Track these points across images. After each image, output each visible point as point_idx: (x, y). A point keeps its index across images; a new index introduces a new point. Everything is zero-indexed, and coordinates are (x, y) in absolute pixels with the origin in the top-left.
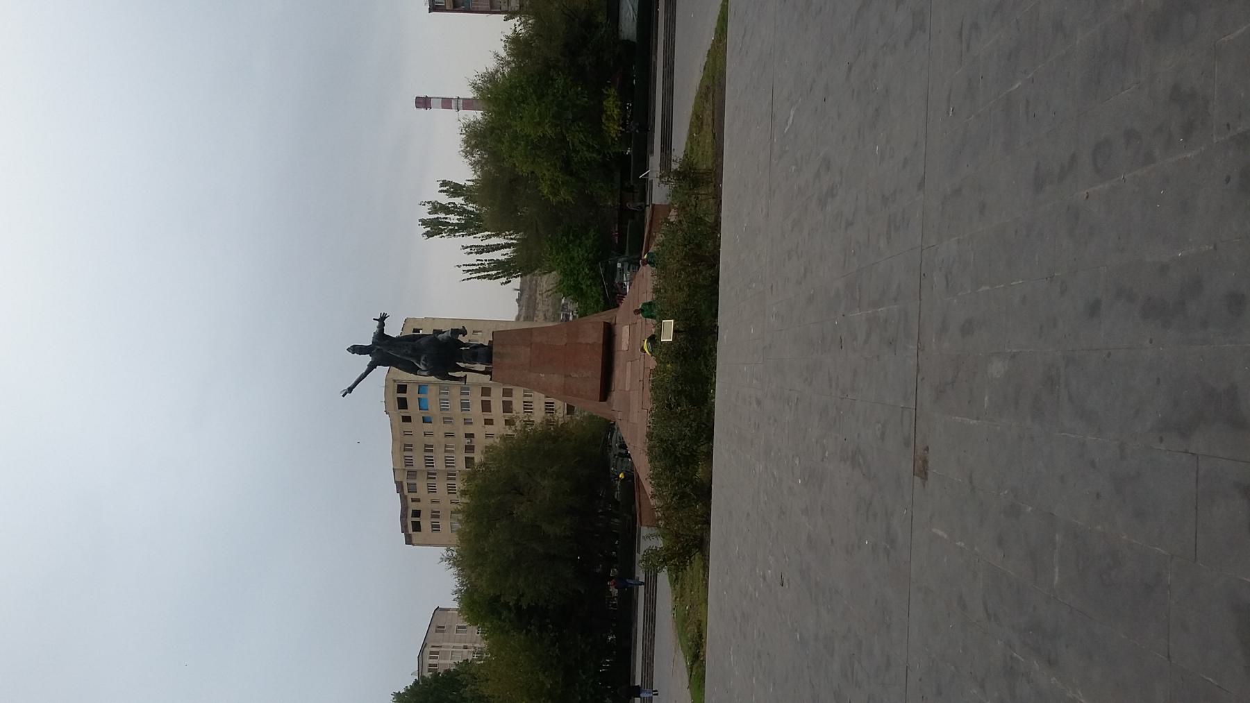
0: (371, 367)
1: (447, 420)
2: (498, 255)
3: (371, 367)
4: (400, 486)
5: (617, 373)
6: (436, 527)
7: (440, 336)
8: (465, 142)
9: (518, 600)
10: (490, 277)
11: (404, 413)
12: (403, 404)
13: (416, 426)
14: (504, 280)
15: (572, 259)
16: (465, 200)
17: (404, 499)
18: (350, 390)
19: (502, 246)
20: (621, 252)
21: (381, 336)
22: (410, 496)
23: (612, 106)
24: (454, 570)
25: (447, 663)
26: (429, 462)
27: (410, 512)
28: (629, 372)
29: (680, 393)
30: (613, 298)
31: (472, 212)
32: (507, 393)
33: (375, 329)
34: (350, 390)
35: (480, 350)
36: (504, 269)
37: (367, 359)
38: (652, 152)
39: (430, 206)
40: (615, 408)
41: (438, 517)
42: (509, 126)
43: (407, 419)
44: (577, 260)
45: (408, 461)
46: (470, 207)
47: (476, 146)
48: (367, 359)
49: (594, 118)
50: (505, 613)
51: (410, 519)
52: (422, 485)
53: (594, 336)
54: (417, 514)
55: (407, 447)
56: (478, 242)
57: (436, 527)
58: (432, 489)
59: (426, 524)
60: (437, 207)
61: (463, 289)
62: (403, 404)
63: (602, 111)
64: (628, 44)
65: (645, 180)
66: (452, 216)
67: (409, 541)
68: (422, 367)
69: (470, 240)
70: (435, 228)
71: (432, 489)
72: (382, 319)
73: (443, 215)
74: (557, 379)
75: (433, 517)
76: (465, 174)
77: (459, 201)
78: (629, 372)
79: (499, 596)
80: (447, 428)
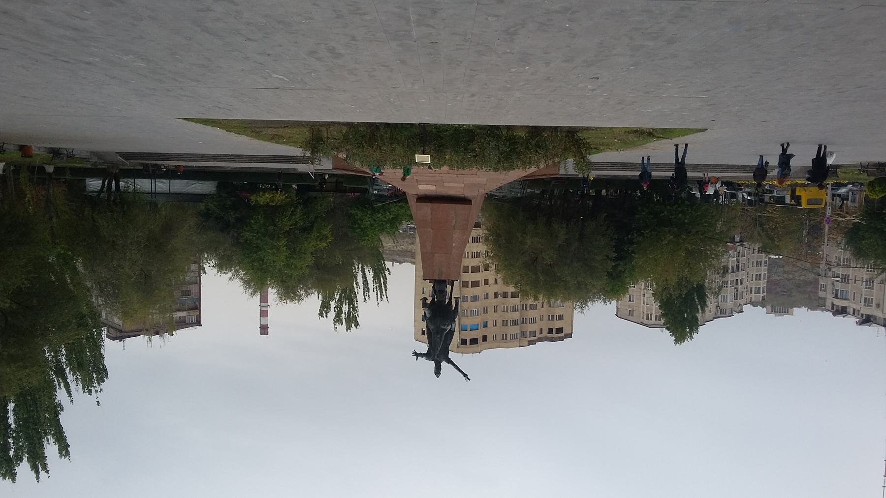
0: (449, 361)
1: (485, 311)
2: (370, 277)
3: (449, 361)
5: (452, 193)
6: (560, 318)
7: (428, 315)
8: (292, 300)
9: (611, 259)
10: (385, 282)
11: (480, 340)
12: (474, 341)
13: (490, 332)
14: (387, 273)
15: (371, 225)
16: (332, 300)
17: (540, 340)
18: (465, 375)
19: (363, 274)
20: (366, 190)
21: (428, 356)
22: (538, 335)
23: (263, 199)
24: (589, 304)
25: (655, 308)
26: (514, 323)
27: (550, 335)
28: (451, 185)
29: (466, 149)
30: (399, 197)
31: (341, 295)
32: (466, 270)
33: (424, 359)
34: (465, 375)
35: (437, 288)
36: (380, 273)
37: (444, 364)
38: (295, 170)
39: (337, 324)
40: (476, 194)
42: (280, 270)
43: (485, 338)
44: (372, 222)
45: (514, 337)
46: (337, 297)
47: (295, 293)
48: (444, 364)
49: (272, 212)
50: (620, 268)
51: (555, 335)
52: (531, 327)
53: (427, 209)
54: (550, 331)
55: (504, 338)
56: (361, 291)
57: (560, 318)
58: (533, 321)
59: (558, 324)
60: (338, 319)
61: (394, 301)
62: (474, 341)
63: (267, 205)
64: (219, 187)
65: (315, 175)
66: (344, 309)
67: (569, 336)
68: (449, 328)
69: (360, 297)
70: (352, 321)
71: (533, 321)
72: (416, 354)
73: (343, 315)
74: (457, 235)
75: (552, 320)
76: (314, 301)
77: (333, 304)
78: (451, 185)
79: (608, 273)
80: (491, 310)
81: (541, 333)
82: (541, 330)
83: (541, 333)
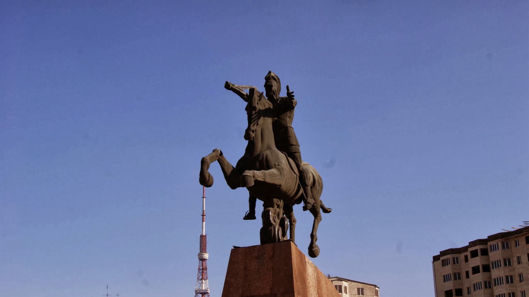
4: (473, 244)
6: (446, 278)
17: (465, 249)
18: (227, 86)
22: (468, 253)
26: (497, 264)
34: (227, 86)
41: (455, 279)
52: (477, 261)
57: (446, 278)
58: (476, 270)
59: (448, 270)
67: (436, 258)
71: (476, 270)
75: (455, 274)
81: (466, 257)
82: (466, 260)
83: (466, 257)
